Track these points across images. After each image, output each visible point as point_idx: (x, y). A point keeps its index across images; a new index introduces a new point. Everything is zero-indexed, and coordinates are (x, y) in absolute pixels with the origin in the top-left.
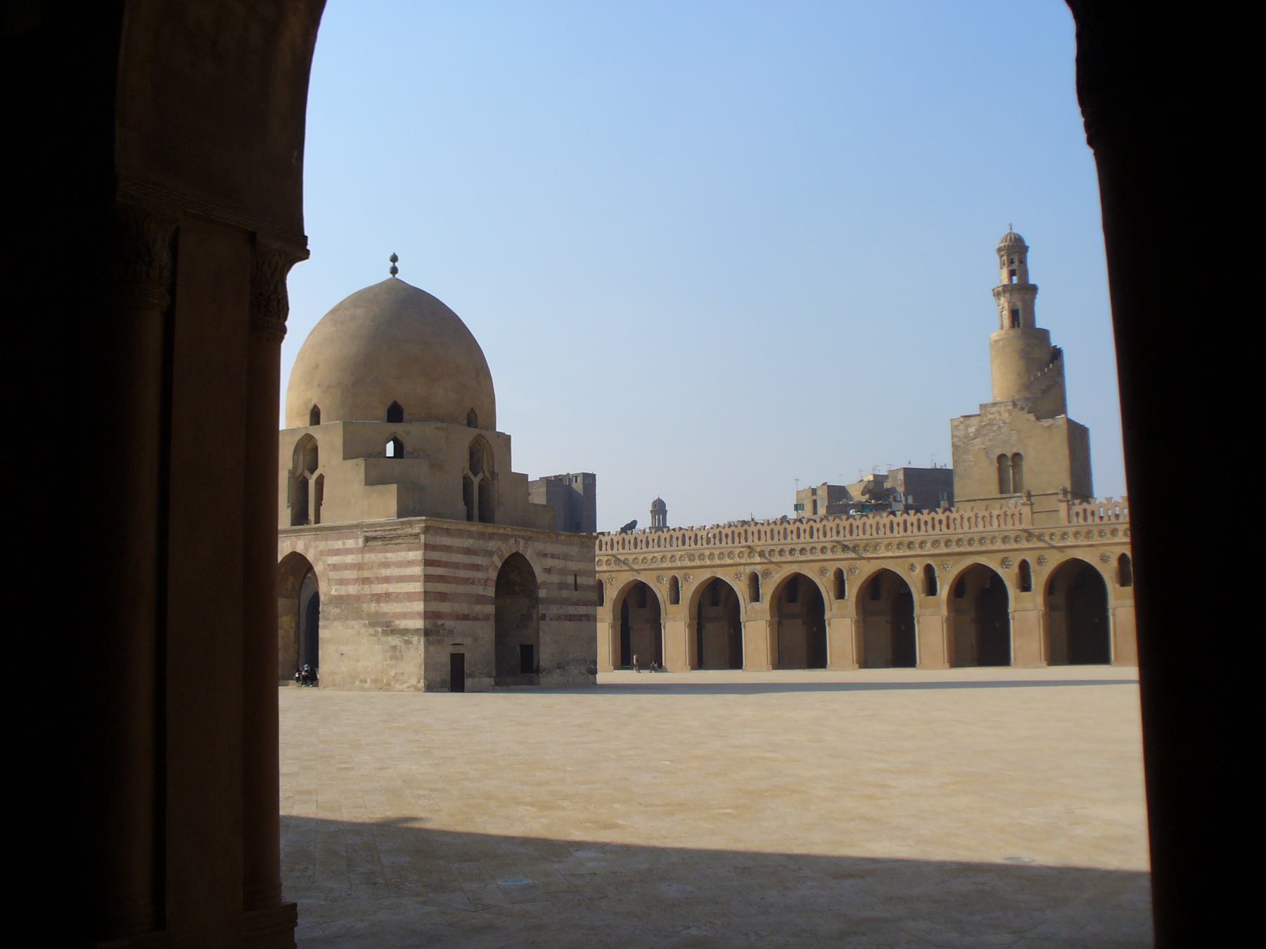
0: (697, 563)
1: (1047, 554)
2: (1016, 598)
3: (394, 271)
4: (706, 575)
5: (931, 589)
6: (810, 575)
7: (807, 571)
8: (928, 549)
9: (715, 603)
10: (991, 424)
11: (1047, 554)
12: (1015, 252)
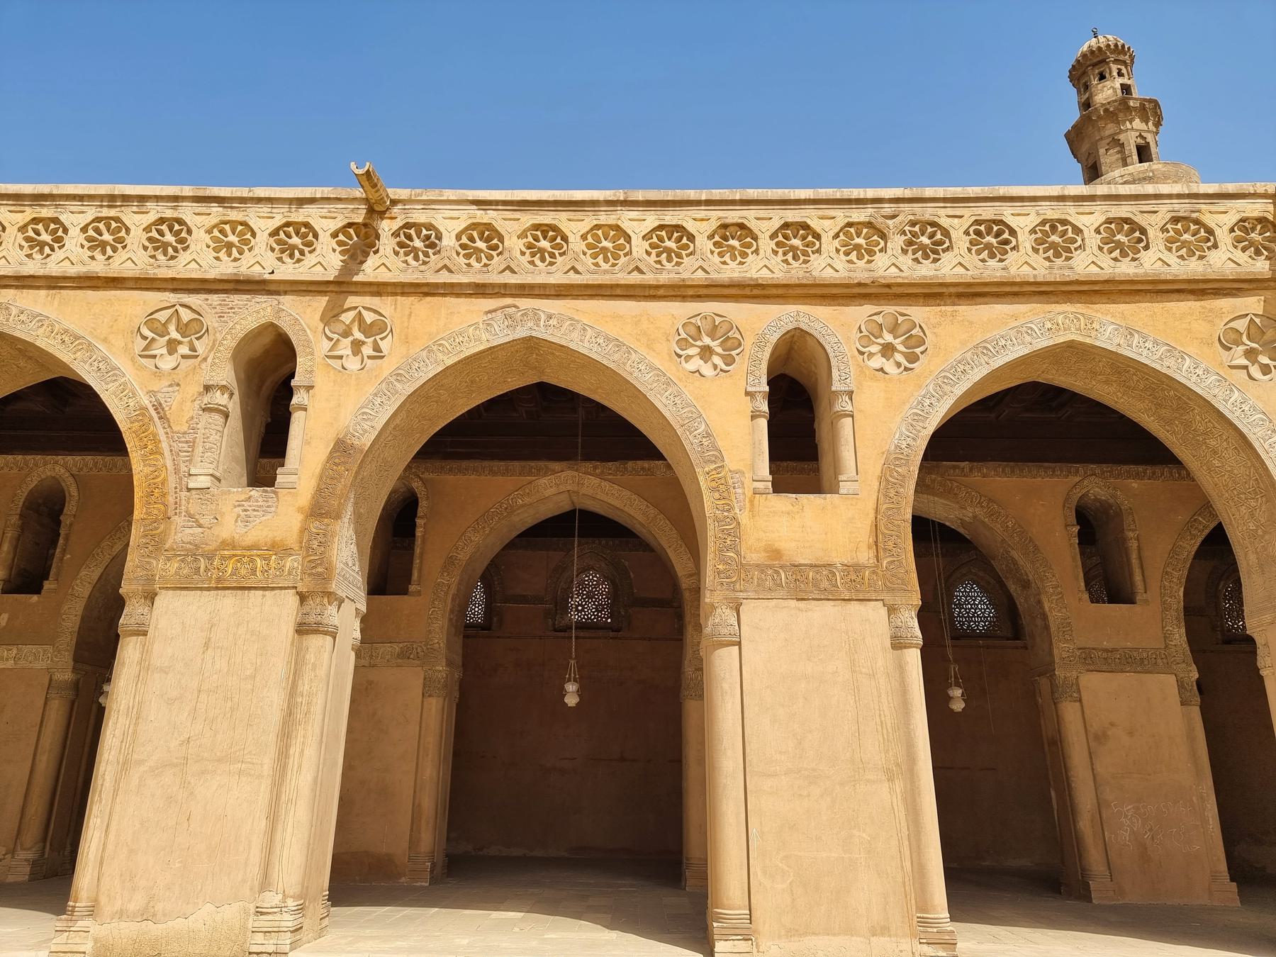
0: (954, 265)
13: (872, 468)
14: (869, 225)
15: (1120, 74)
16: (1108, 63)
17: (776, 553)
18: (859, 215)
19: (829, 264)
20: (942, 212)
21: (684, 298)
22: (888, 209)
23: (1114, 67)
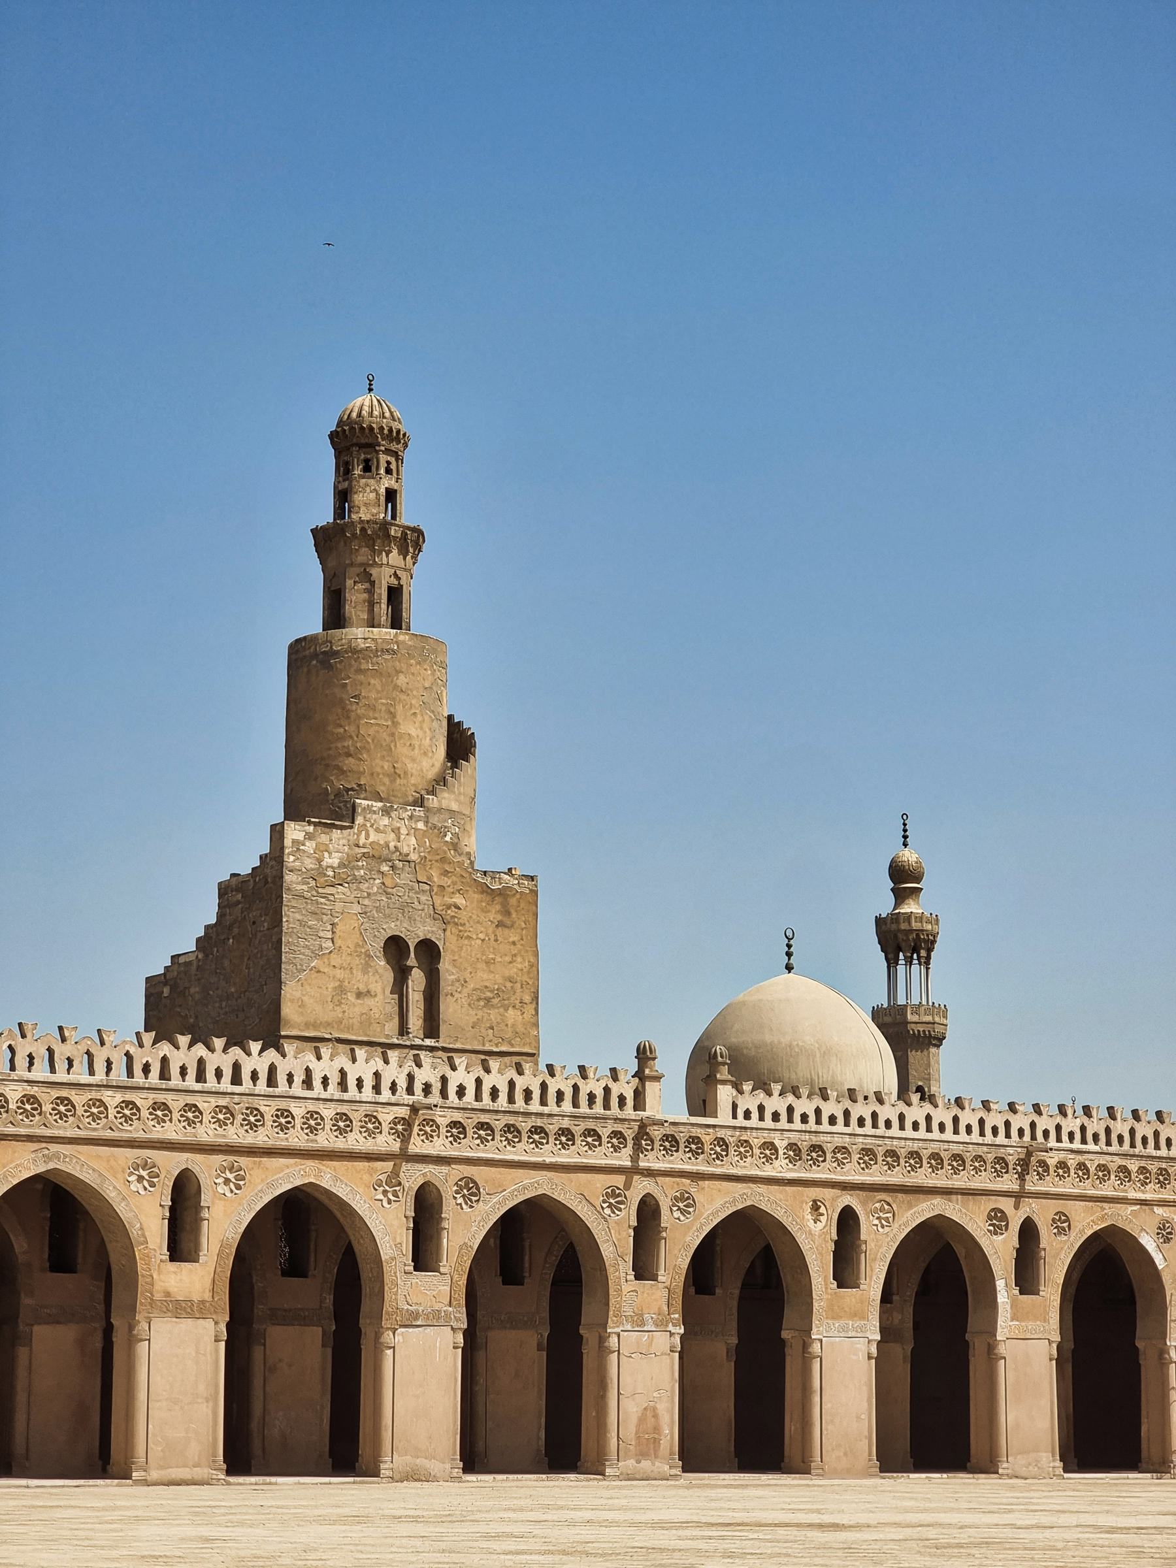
0: (262, 1137)
1: (1076, 1210)
2: (1014, 1304)
4: (286, 1176)
5: (845, 1267)
6: (583, 1211)
7: (567, 1192)
8: (852, 1173)
9: (295, 1268)
11: (1076, 1210)
12: (359, 446)
13: (215, 1249)
14: (226, 1107)
15: (388, 471)
16: (377, 452)
17: (168, 1294)
18: (223, 1102)
19: (206, 1132)
20: (262, 1102)
21: (132, 1147)
22: (237, 1099)
23: (383, 458)
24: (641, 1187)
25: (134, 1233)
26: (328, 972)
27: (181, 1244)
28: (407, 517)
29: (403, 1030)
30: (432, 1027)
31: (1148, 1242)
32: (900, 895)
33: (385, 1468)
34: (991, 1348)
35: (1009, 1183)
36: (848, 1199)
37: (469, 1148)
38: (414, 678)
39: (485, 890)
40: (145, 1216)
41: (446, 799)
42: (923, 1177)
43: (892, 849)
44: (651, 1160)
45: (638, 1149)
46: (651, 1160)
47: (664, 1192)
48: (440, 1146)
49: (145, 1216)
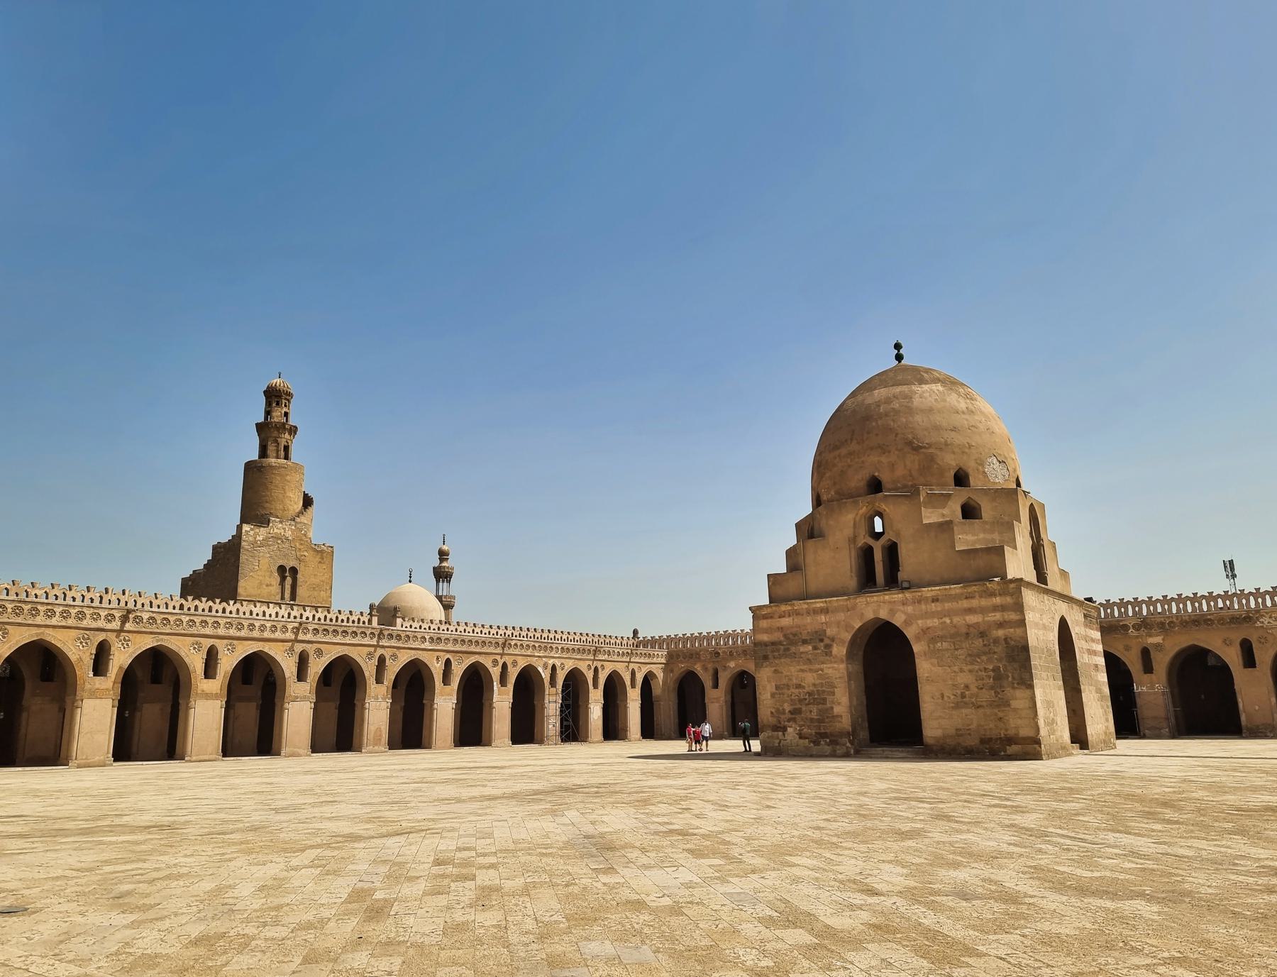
0: (243, 633)
1: (519, 659)
3: (899, 358)
7: (354, 653)
8: (450, 647)
10: (276, 538)
11: (519, 659)
12: (274, 396)
19: (221, 632)
24: (380, 652)
25: (191, 668)
26: (256, 576)
27: (209, 672)
28: (291, 422)
29: (283, 598)
30: (293, 597)
31: (540, 669)
32: (442, 560)
33: (283, 753)
34: (491, 704)
35: (499, 650)
36: (448, 656)
37: (320, 638)
38: (293, 477)
39: (315, 550)
40: (196, 662)
41: (303, 519)
42: (473, 649)
43: (440, 545)
44: (384, 642)
45: (379, 638)
46: (383, 643)
47: (387, 653)
48: (309, 637)
49: (196, 662)
